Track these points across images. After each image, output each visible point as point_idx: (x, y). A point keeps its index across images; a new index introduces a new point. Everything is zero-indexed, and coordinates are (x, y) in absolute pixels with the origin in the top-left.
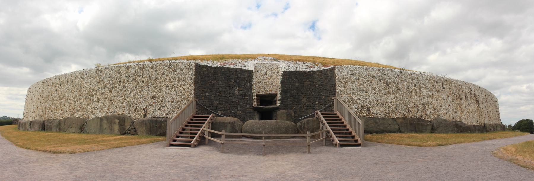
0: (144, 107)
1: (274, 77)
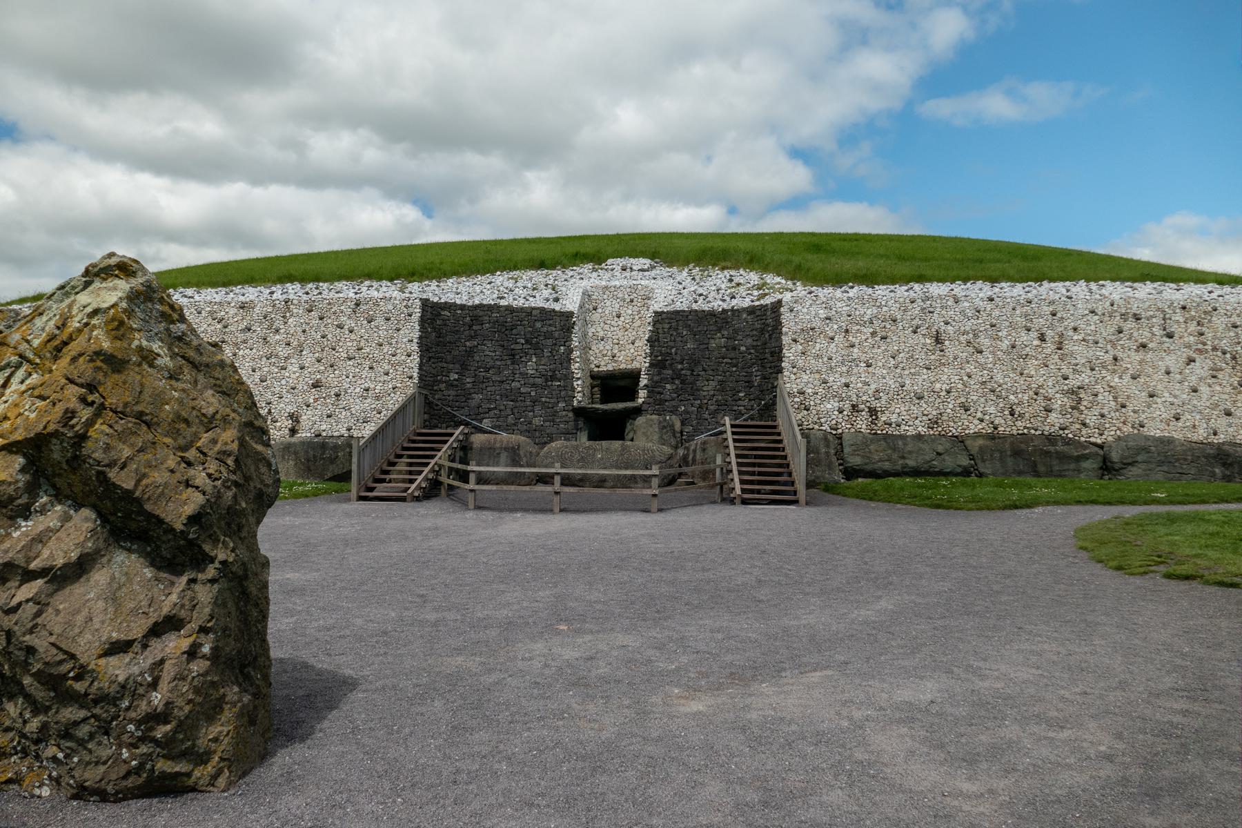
0: (291, 409)
1: (638, 323)
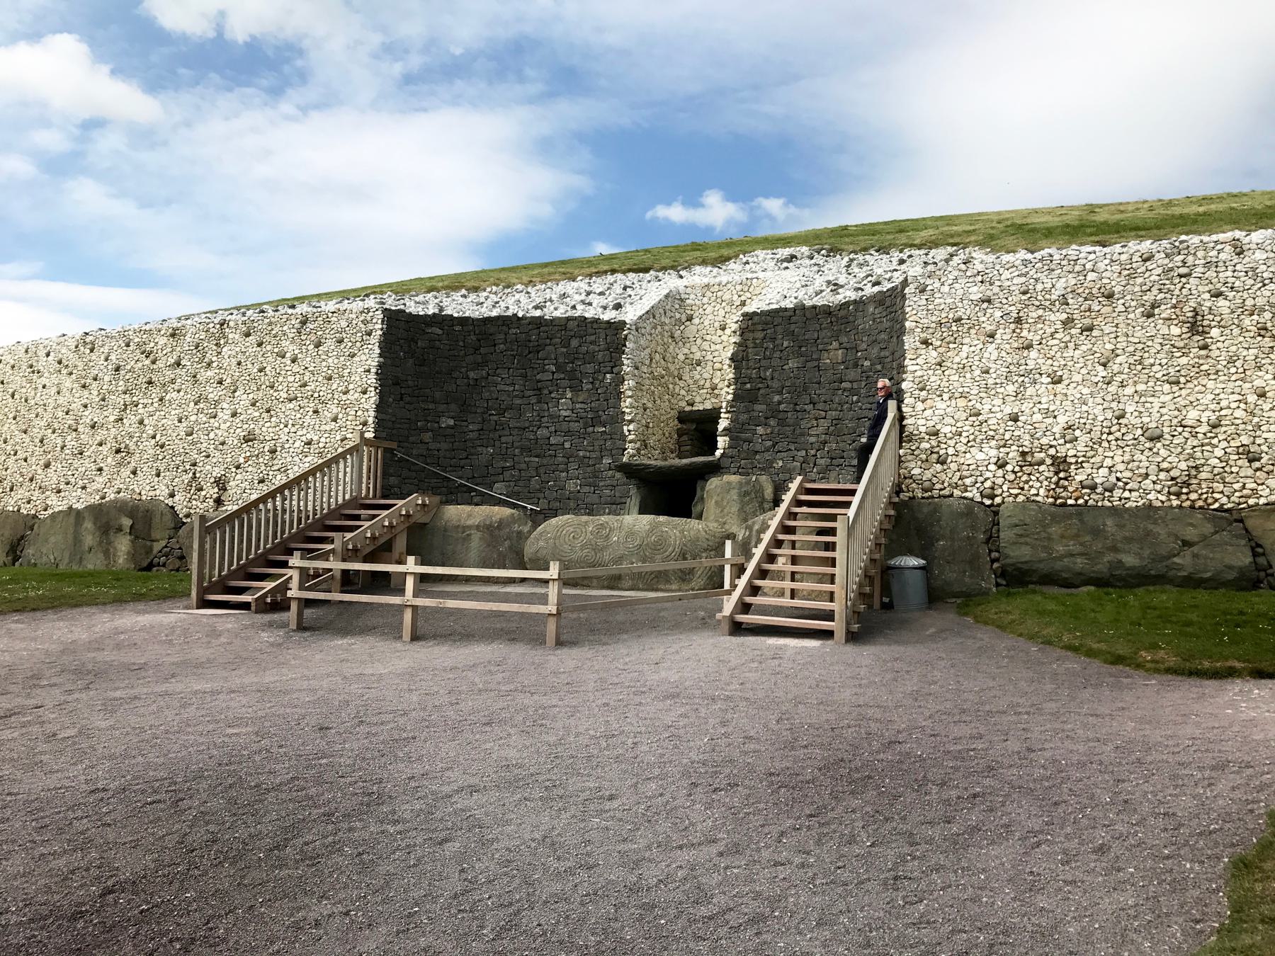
0: (217, 472)
